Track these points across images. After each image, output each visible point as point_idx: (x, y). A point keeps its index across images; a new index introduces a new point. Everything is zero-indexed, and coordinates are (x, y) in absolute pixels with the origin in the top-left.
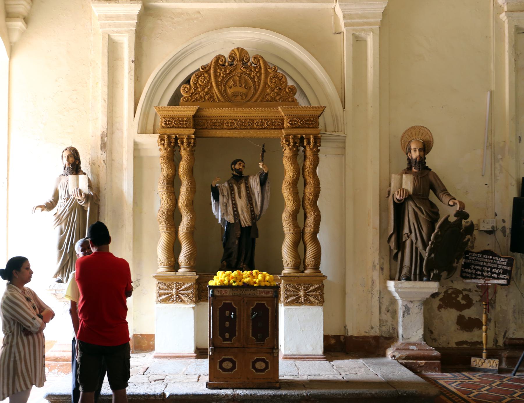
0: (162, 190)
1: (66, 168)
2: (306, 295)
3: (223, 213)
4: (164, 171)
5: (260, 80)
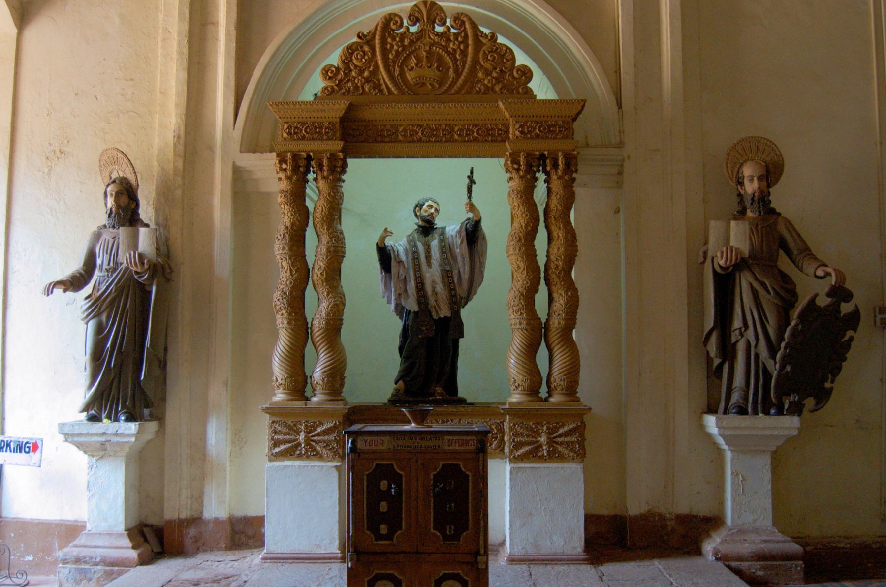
0: (281, 252)
1: (113, 215)
2: (551, 442)
3: (400, 295)
4: (287, 217)
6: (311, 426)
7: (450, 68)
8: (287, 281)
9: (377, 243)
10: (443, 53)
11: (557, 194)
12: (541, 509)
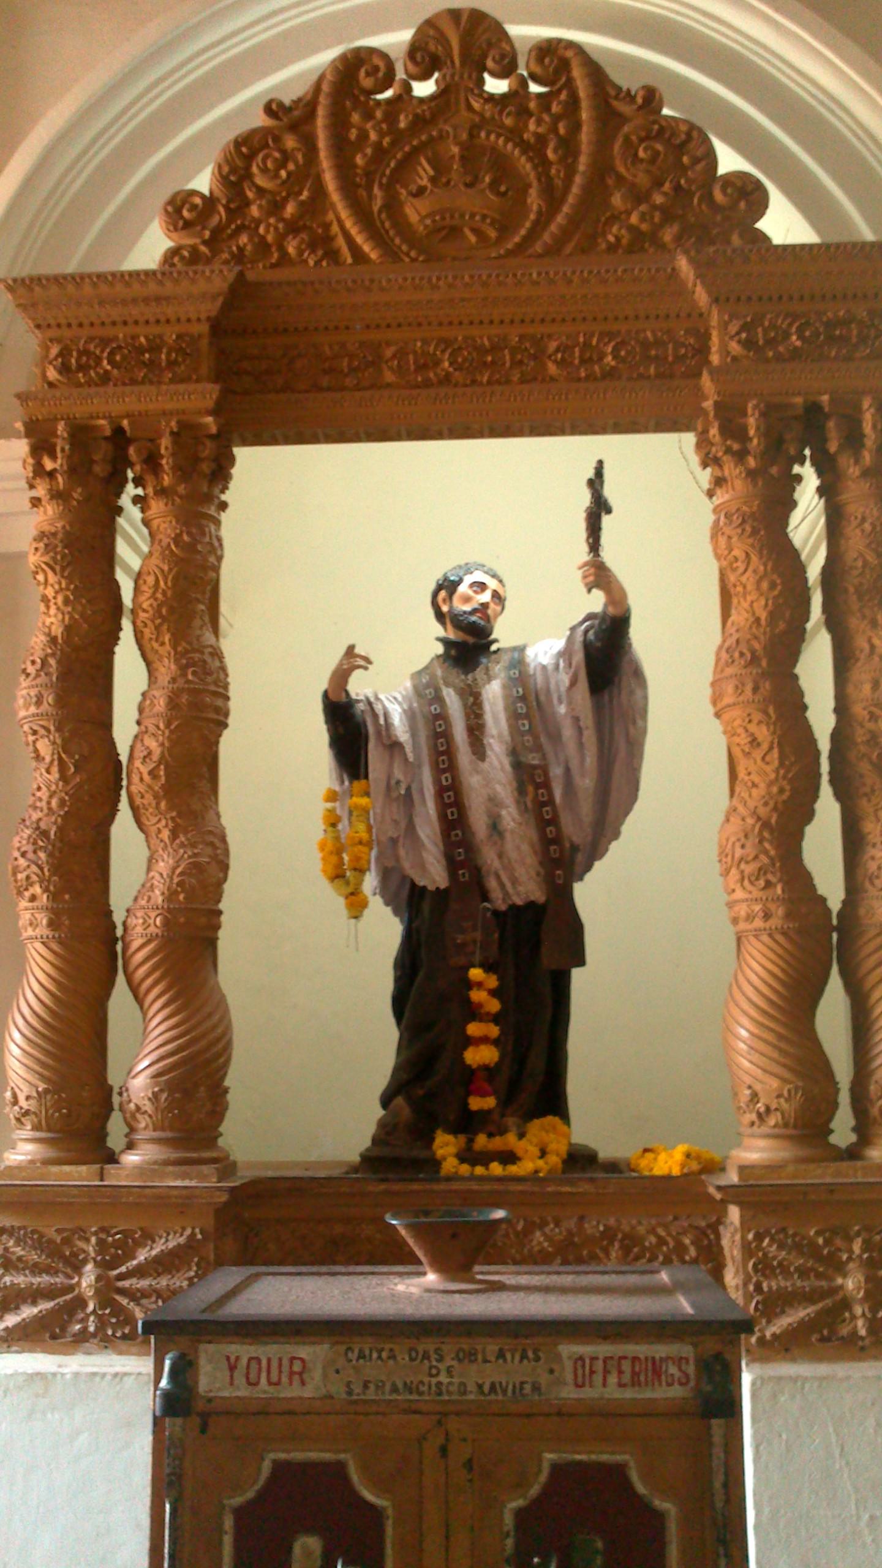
0: (33, 709)
4: (53, 611)
6: (117, 1245)
7: (529, 186)
8: (51, 797)
9: (326, 695)
10: (510, 146)
11: (864, 520)
12: (859, 1518)
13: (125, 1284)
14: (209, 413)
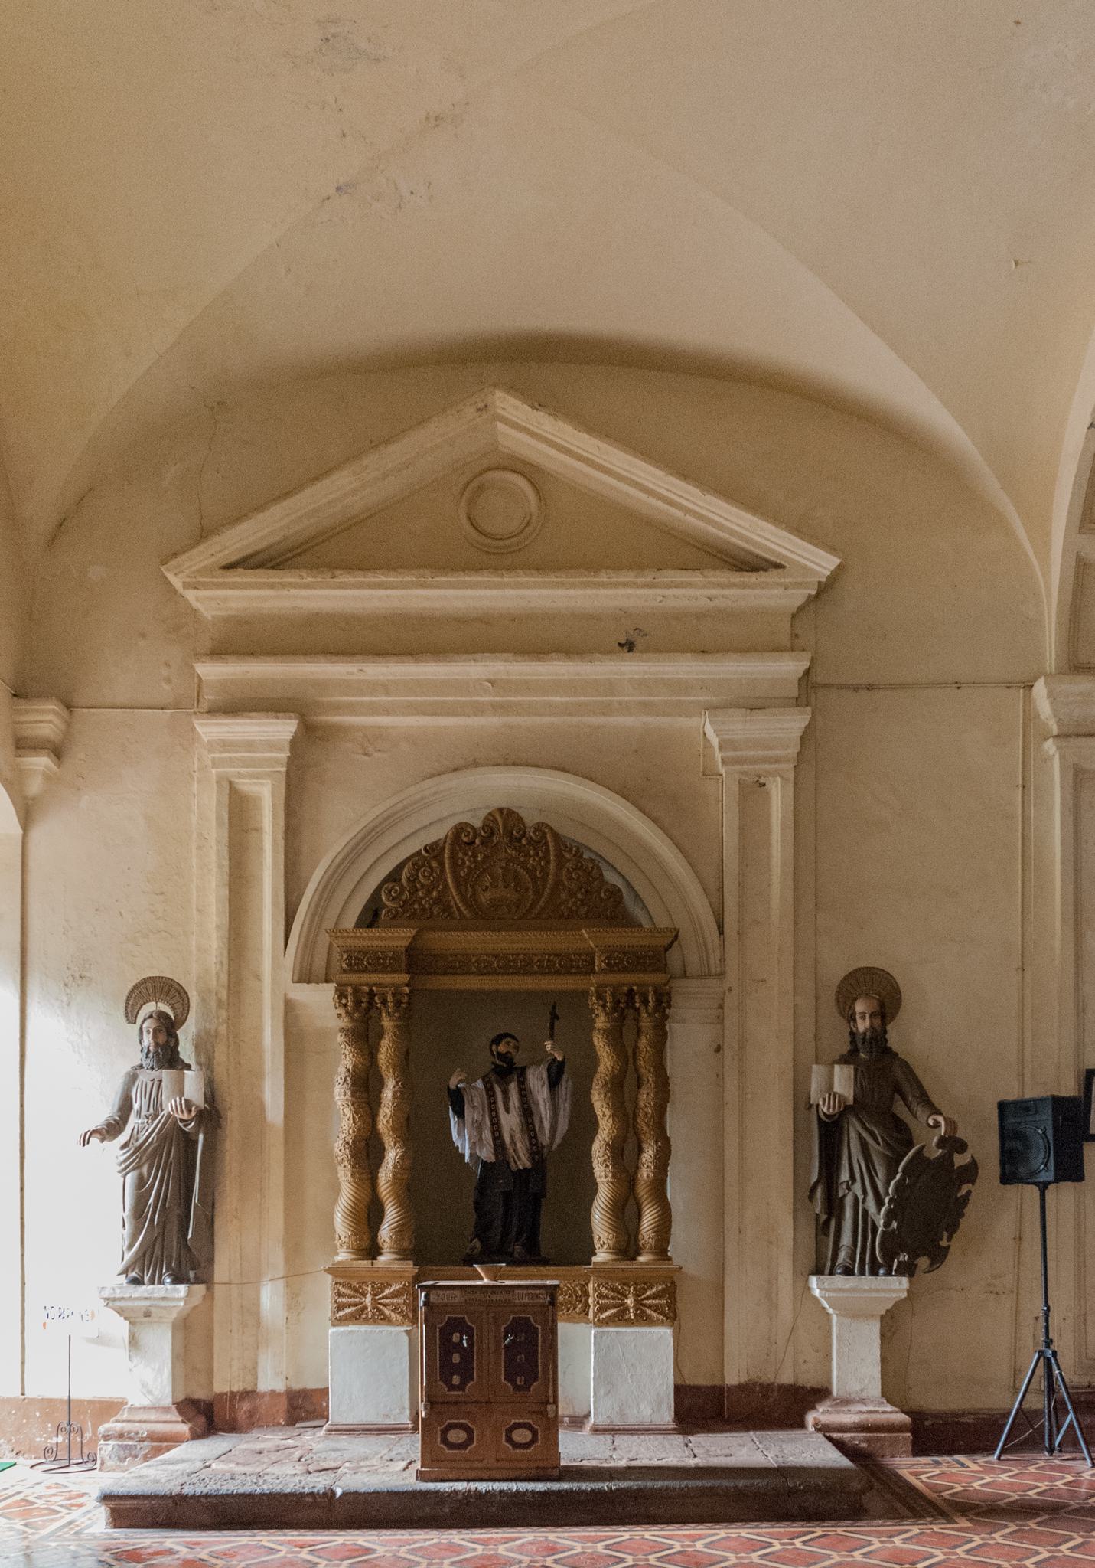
0: (342, 1097)
2: (639, 1304)
3: (474, 1143)
4: (348, 1059)
5: (547, 874)
13: (382, 1301)
14: (407, 985)
